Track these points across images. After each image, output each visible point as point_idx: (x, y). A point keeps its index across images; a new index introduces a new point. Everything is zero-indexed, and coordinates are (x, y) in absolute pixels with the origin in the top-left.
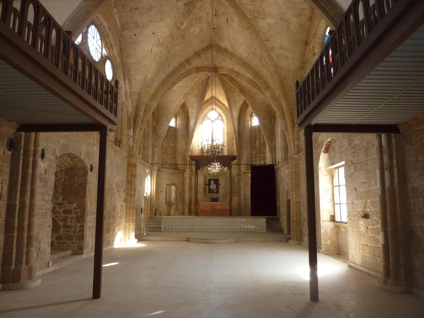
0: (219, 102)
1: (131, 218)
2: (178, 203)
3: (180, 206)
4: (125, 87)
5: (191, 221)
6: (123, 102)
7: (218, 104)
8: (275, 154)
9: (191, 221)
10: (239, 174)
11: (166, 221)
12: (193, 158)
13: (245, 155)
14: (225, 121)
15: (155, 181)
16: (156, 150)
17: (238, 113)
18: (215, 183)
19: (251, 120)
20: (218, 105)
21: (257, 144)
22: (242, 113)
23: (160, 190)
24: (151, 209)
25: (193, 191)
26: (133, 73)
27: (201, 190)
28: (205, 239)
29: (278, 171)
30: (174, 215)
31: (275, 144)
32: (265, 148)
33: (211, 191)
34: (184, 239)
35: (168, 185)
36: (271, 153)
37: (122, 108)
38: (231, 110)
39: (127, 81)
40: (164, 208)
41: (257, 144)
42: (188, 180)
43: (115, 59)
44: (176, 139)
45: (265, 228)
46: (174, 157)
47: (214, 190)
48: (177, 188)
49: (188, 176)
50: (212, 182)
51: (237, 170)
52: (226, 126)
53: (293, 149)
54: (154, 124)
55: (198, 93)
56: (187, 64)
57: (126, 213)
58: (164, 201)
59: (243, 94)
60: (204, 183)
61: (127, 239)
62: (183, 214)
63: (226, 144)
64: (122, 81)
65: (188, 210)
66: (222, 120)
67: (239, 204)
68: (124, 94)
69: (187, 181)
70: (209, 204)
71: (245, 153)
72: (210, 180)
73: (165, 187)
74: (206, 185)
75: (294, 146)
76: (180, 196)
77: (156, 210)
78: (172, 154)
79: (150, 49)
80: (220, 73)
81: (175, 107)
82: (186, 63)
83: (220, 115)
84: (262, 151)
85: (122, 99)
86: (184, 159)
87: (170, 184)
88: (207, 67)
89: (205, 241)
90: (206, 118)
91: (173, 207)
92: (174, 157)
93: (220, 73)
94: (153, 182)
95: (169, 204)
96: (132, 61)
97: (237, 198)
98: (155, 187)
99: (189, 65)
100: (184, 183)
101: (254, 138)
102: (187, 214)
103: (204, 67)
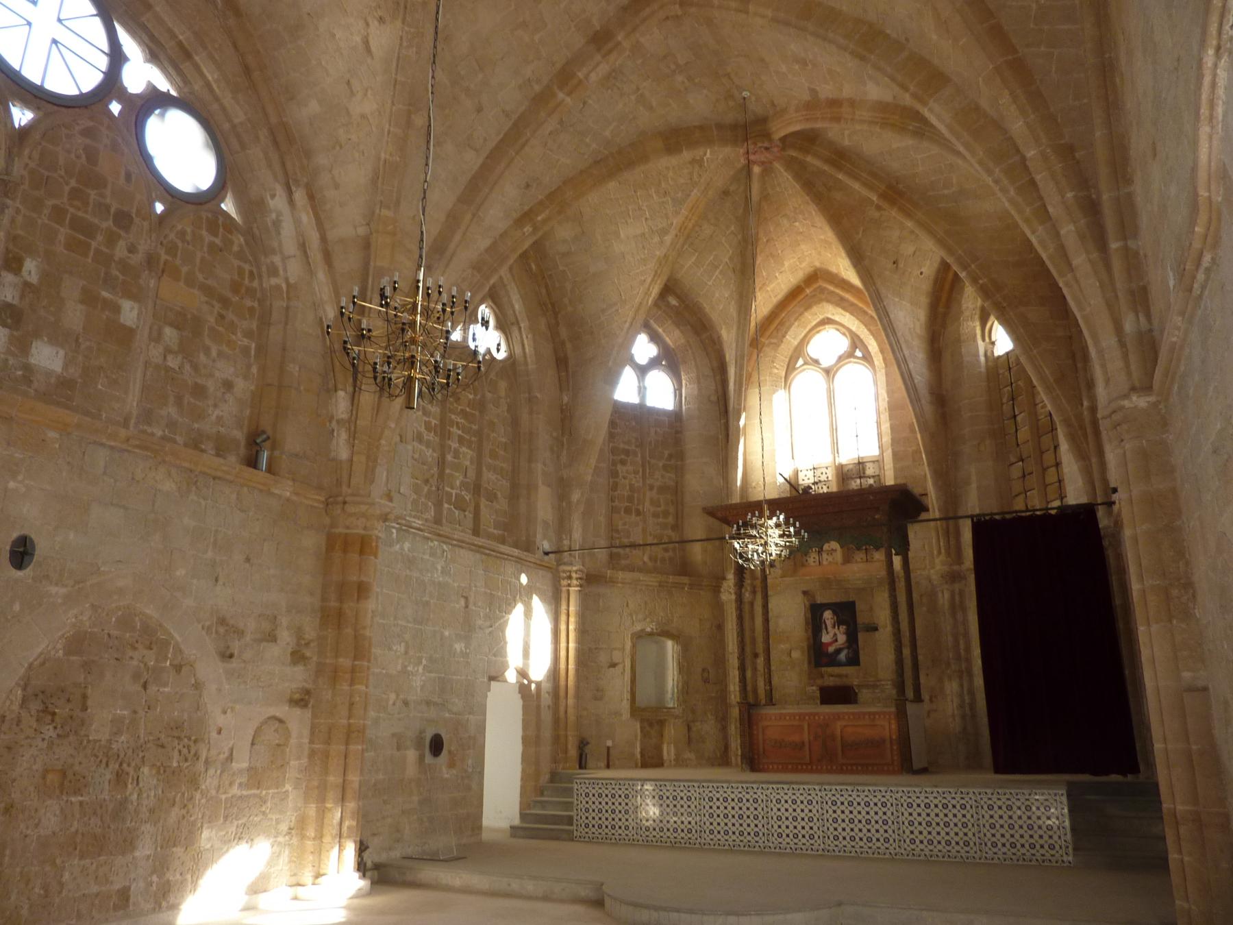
0: (843, 288)
1: (331, 779)
2: (693, 711)
3: (708, 728)
4: (297, 222)
5: (694, 794)
6: (292, 281)
7: (842, 299)
9: (694, 794)
13: (974, 485)
14: (878, 360)
15: (572, 619)
16: (576, 496)
17: (922, 315)
18: (839, 622)
19: (987, 334)
20: (841, 303)
21: (1024, 433)
22: (941, 310)
23: (603, 658)
24: (556, 739)
26: (322, 160)
28: (647, 907)
30: (680, 762)
34: (583, 892)
35: (639, 636)
36: (1081, 455)
37: (288, 308)
38: (877, 300)
39: (300, 195)
40: (627, 733)
41: (1024, 433)
43: (224, 109)
44: (680, 455)
47: (838, 651)
50: (828, 615)
51: (943, 557)
52: (884, 378)
53: (1115, 364)
54: (566, 399)
55: (731, 259)
56: (561, 88)
57: (312, 753)
58: (626, 705)
59: (902, 210)
61: (307, 877)
62: (723, 760)
64: (273, 196)
66: (867, 358)
68: (290, 247)
70: (802, 716)
71: (974, 478)
73: (628, 645)
75: (1122, 344)
76: (706, 681)
77: (583, 744)
78: (666, 514)
79: (358, 39)
80: (777, 136)
81: (629, 320)
82: (555, 87)
83: (856, 342)
84: (1049, 458)
85: (285, 270)
87: (651, 634)
88: (720, 127)
90: (801, 362)
91: (672, 731)
92: (676, 527)
93: (777, 136)
94: (563, 627)
95: (651, 718)
96: (308, 110)
98: (572, 645)
99: (569, 94)
100: (720, 627)
101: (1007, 408)
103: (701, 128)
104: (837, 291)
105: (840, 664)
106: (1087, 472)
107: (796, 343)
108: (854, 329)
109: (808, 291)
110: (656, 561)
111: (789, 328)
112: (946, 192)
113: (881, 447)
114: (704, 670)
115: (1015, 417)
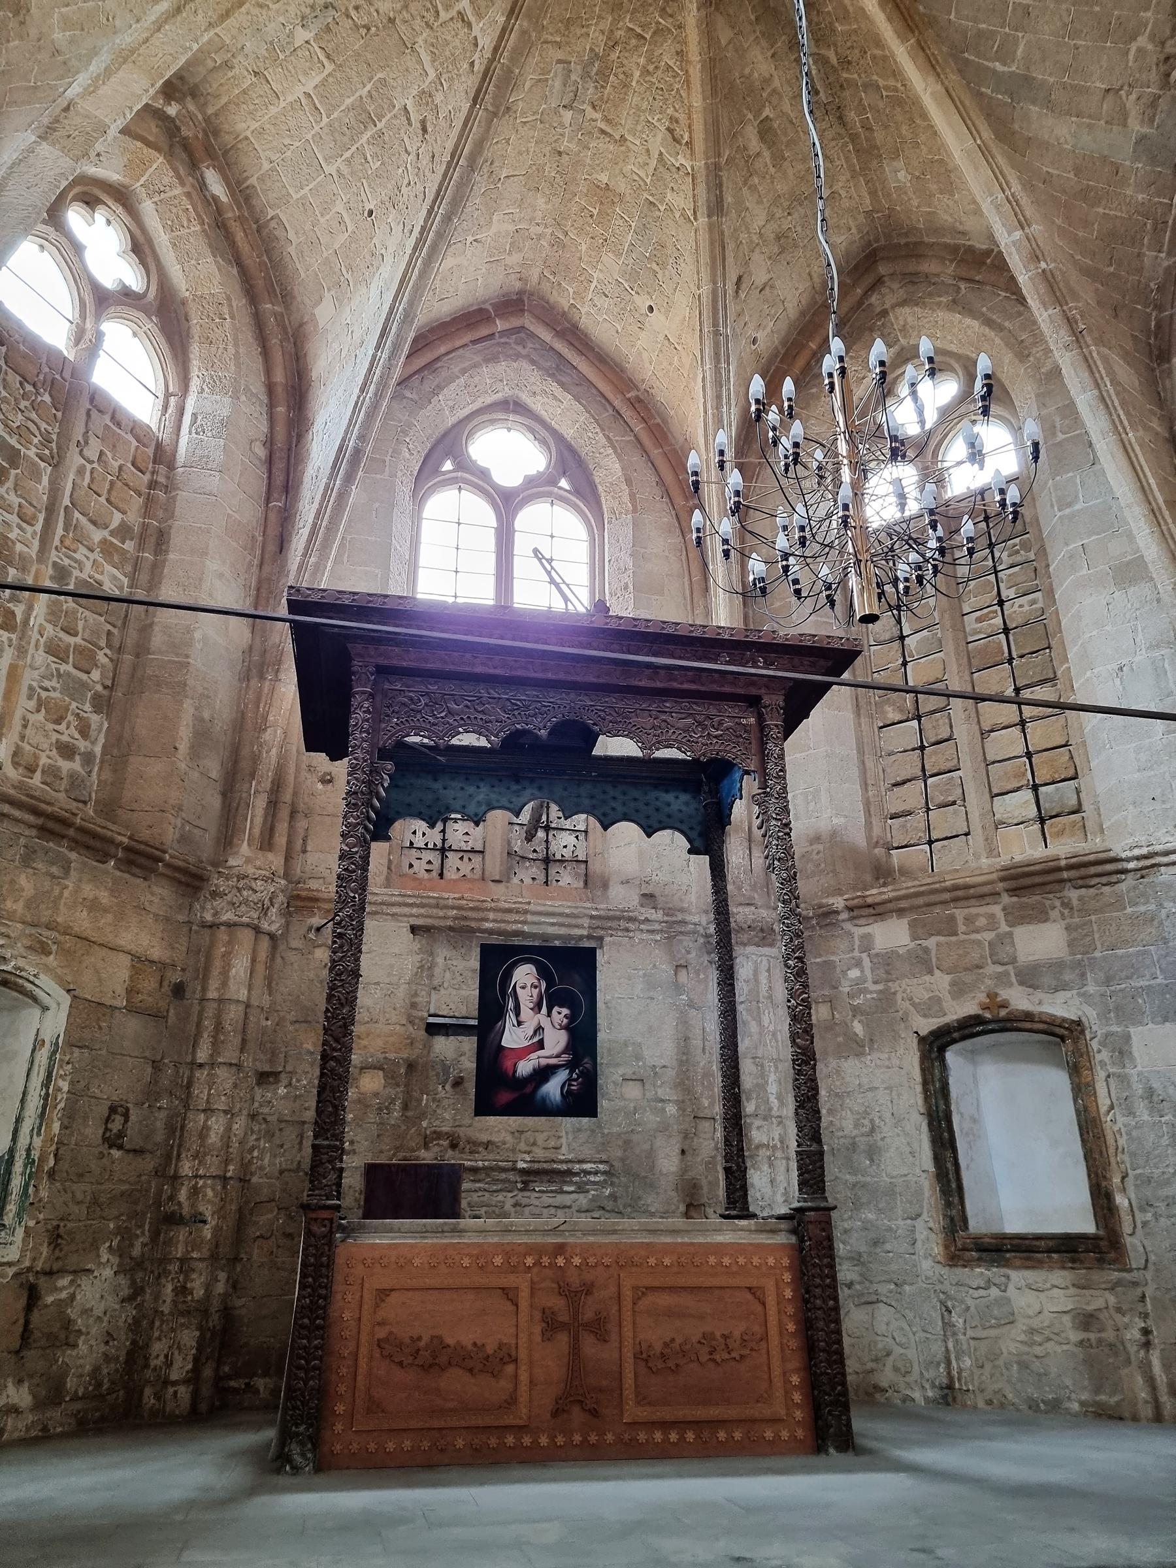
18: (552, 999)
46: (101, 704)
47: (543, 1074)
50: (524, 976)
66: (586, 494)
78: (86, 660)
90: (448, 466)
104: (559, 346)
105: (544, 1109)
107: (451, 421)
108: (569, 433)
109: (500, 325)
110: (31, 770)
111: (452, 379)
112: (998, 66)
114: (113, 1110)
115: (902, 638)
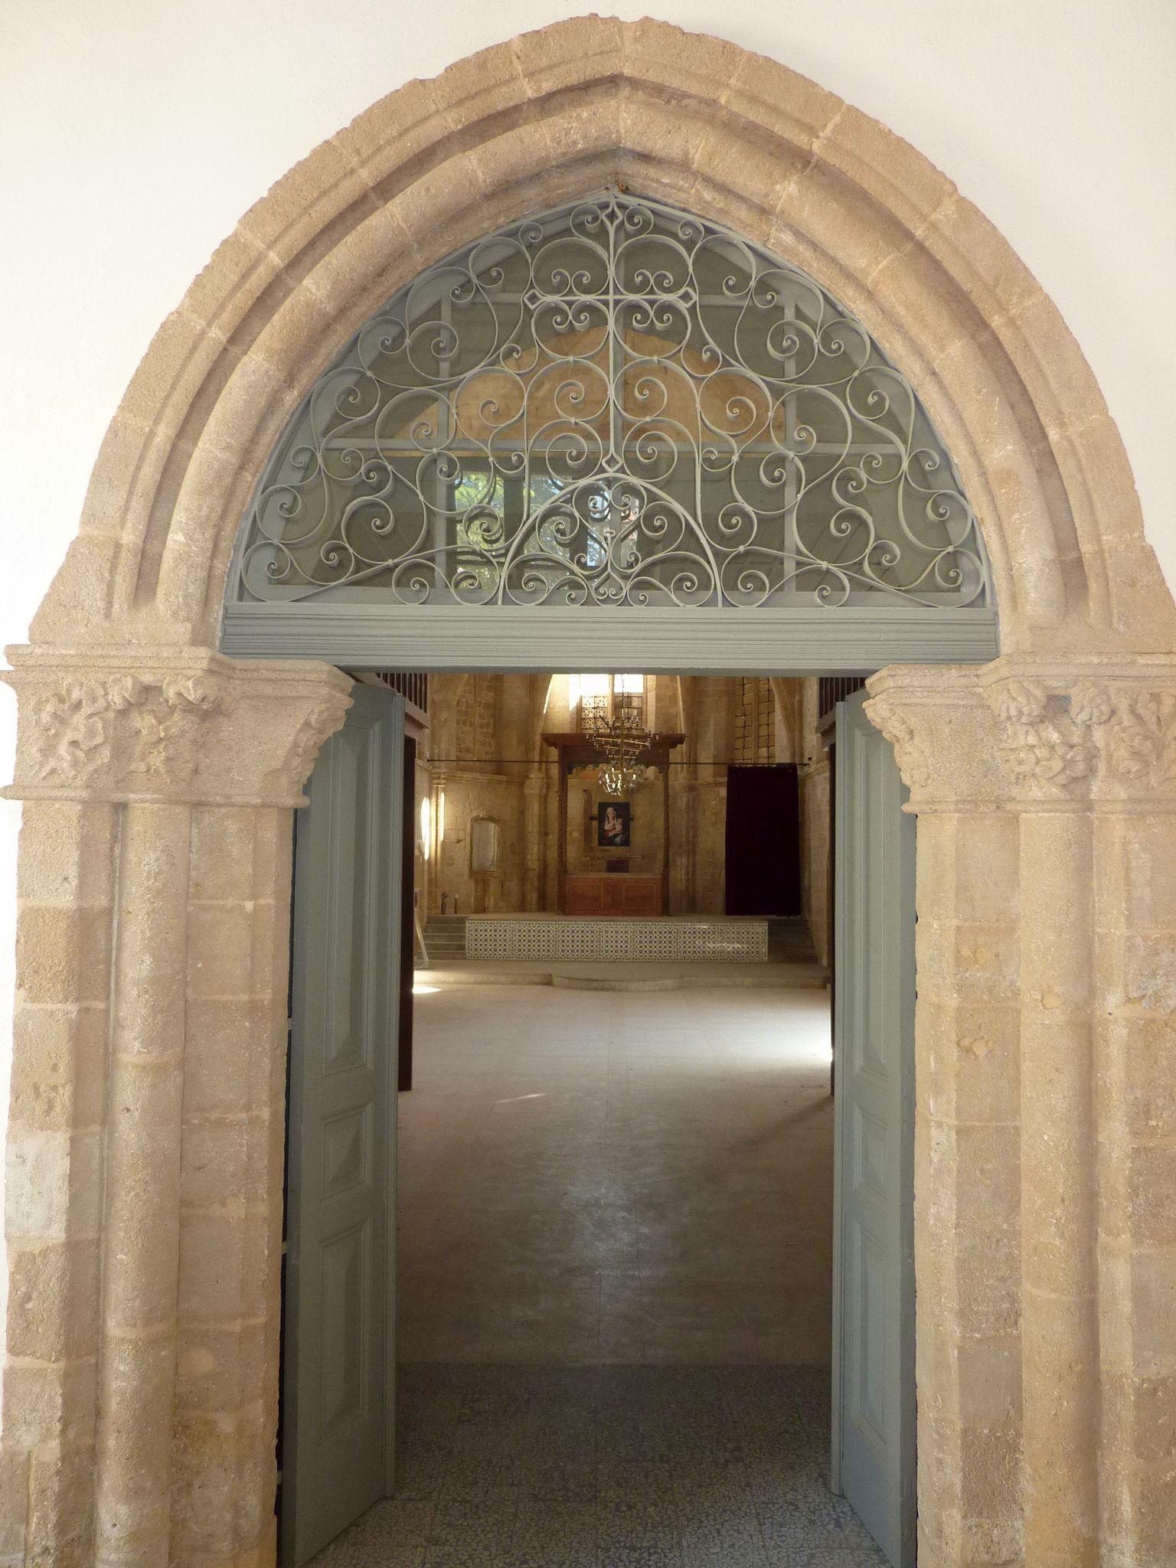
3: (513, 885)
8: (801, 730)
10: (691, 788)
11: (478, 929)
12: (550, 740)
13: (712, 728)
16: (444, 716)
18: (618, 816)
24: (430, 893)
25: (553, 838)
27: (576, 834)
29: (809, 783)
30: (497, 910)
31: (801, 702)
32: (771, 712)
33: (605, 840)
34: (537, 980)
36: (790, 729)
40: (465, 890)
41: (749, 697)
42: (536, 806)
45: (765, 949)
46: (493, 736)
47: (615, 836)
48: (502, 830)
49: (536, 791)
50: (610, 810)
58: (466, 869)
60: (586, 811)
63: (652, 697)
65: (535, 895)
67: (692, 877)
69: (535, 808)
72: (603, 807)
74: (592, 819)
76: (513, 852)
77: (444, 896)
78: (488, 724)
84: (763, 719)
86: (526, 741)
89: (595, 984)
91: (494, 888)
95: (480, 877)
97: (684, 860)
100: (522, 813)
102: (535, 907)
106: (792, 741)
113: (645, 688)
